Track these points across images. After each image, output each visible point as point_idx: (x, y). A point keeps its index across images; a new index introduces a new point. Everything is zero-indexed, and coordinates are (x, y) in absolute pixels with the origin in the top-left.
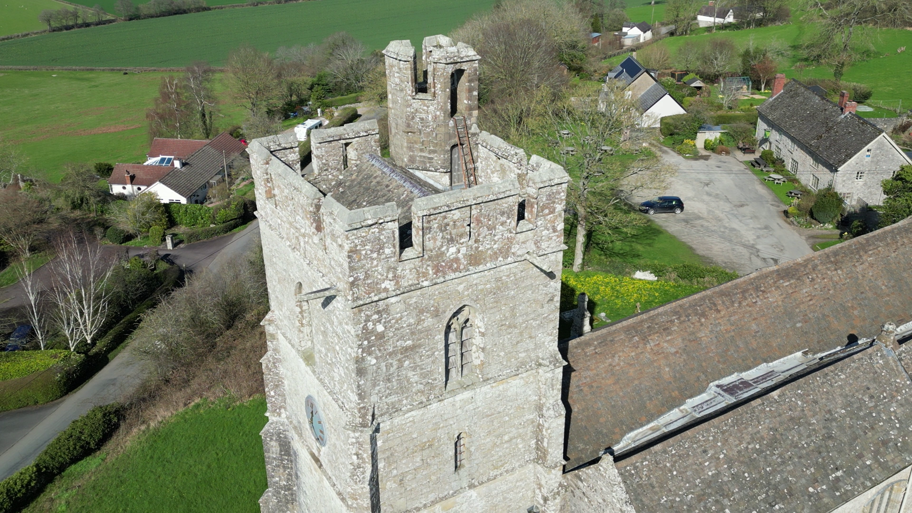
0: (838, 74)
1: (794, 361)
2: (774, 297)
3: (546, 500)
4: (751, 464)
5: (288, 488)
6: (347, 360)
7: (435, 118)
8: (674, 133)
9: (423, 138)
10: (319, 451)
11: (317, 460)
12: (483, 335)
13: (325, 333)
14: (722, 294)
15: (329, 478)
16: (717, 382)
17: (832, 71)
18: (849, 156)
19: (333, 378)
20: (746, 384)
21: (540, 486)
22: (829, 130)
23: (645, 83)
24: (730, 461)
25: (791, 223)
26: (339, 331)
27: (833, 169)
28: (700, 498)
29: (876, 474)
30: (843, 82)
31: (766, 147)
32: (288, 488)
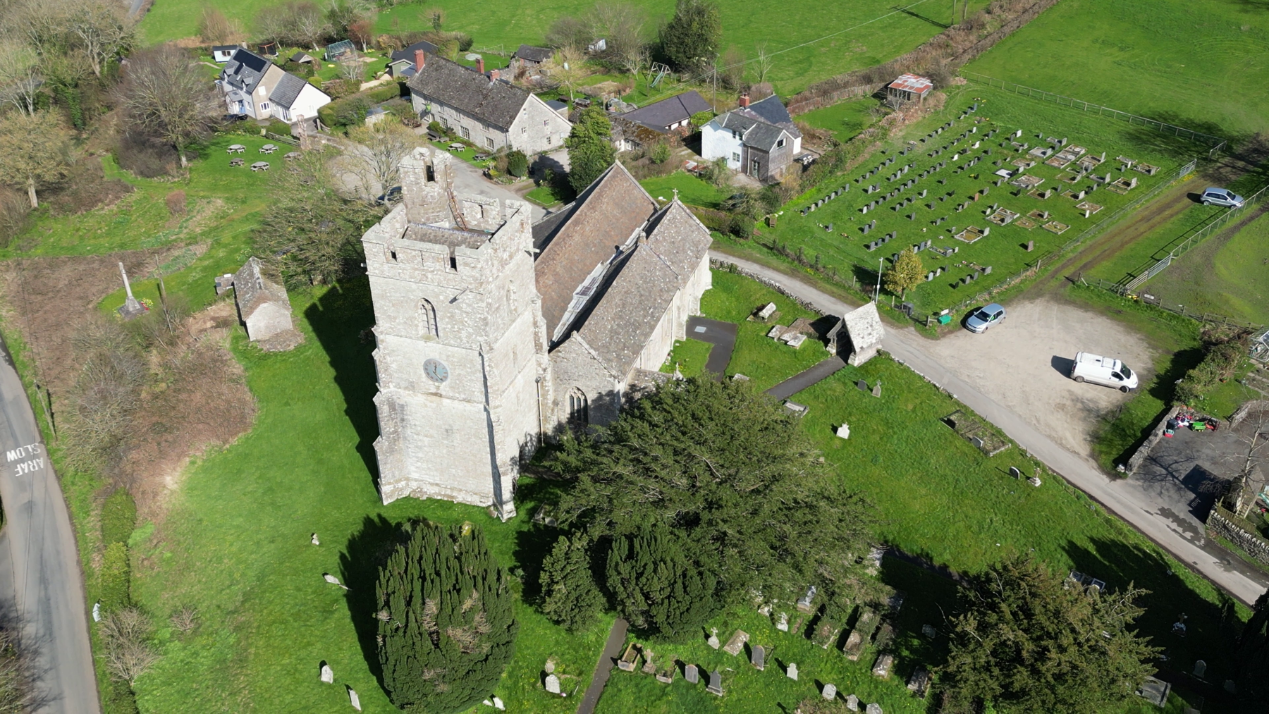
0: (437, 25)
2: (577, 238)
3: (545, 370)
4: (621, 317)
5: (395, 432)
8: (339, 120)
10: (438, 388)
11: (436, 394)
13: (452, 317)
15: (452, 398)
16: (579, 289)
17: (431, 24)
18: (513, 118)
20: (588, 288)
21: (540, 365)
22: (486, 97)
23: (274, 75)
25: (497, 183)
26: (469, 310)
27: (504, 130)
28: (611, 338)
29: (664, 305)
30: (444, 34)
31: (429, 120)
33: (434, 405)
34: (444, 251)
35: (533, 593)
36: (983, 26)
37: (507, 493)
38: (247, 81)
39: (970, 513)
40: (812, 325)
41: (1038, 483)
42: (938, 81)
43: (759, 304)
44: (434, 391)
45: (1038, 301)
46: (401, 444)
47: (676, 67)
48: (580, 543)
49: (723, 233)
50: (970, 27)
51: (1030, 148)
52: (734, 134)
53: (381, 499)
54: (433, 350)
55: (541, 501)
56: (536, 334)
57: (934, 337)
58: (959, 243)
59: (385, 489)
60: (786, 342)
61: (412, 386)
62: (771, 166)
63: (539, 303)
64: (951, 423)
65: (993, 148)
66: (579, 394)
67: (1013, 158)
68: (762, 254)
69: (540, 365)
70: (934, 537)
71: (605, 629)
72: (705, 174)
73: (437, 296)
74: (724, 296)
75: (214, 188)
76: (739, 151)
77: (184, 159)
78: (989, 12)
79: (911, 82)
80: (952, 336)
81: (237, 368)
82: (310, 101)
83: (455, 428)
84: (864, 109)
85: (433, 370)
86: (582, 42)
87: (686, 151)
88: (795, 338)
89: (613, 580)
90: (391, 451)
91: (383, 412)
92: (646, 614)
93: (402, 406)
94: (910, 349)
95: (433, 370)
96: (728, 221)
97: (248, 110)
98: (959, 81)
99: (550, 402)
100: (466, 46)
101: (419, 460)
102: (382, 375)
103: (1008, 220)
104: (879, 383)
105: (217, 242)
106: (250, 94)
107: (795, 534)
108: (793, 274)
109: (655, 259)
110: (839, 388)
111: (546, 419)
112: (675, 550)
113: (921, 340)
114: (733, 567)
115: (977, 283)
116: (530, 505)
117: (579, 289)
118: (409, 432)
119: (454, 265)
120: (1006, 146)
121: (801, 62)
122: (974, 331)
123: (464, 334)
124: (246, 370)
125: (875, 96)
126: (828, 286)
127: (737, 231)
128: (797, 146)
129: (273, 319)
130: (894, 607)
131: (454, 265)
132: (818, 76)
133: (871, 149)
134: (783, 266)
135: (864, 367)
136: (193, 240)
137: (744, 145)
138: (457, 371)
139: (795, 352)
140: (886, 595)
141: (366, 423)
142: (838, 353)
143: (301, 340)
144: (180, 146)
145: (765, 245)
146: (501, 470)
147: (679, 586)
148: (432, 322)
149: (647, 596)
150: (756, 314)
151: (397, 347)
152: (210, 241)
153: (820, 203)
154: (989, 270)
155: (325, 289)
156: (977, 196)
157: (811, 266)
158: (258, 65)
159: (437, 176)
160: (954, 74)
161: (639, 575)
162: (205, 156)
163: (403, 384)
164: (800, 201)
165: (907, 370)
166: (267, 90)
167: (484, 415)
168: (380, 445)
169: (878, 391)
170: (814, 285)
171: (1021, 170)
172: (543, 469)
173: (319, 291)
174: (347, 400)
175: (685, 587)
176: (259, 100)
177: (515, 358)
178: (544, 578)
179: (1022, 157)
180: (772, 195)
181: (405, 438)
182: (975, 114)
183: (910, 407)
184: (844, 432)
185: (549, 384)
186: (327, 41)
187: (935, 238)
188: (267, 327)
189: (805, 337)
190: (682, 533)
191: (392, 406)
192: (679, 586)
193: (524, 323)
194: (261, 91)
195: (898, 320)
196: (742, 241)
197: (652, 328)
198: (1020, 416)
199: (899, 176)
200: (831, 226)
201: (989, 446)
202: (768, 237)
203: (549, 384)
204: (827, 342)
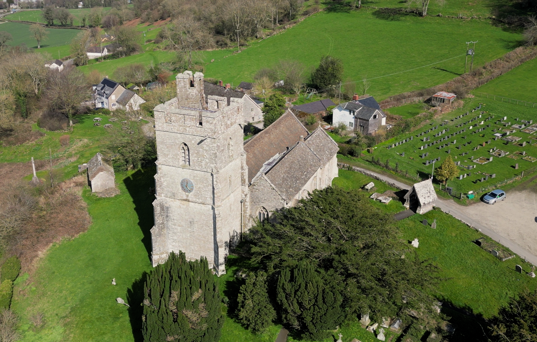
1: (277, 156)
3: (246, 195)
5: (163, 223)
6: (211, 155)
7: (196, 93)
9: (192, 100)
10: (187, 196)
11: (186, 200)
12: (232, 146)
13: (198, 153)
14: (255, 140)
16: (266, 163)
19: (201, 165)
20: (271, 163)
23: (120, 90)
24: (284, 173)
26: (207, 148)
28: (283, 181)
29: (313, 172)
32: (163, 223)
33: (185, 206)
34: (195, 113)
35: (233, 311)
36: (481, 74)
37: (221, 260)
38: (106, 92)
39: (493, 289)
40: (396, 193)
41: (534, 276)
42: (459, 95)
43: (364, 184)
44: (185, 198)
45: (524, 192)
46: (165, 231)
48: (262, 276)
49: (344, 155)
50: (474, 74)
51: (512, 125)
52: (350, 112)
53: (152, 264)
54: (186, 174)
55: (240, 266)
56: (242, 174)
57: (465, 205)
58: (475, 163)
59: (155, 257)
60: (380, 201)
61: (173, 196)
62: (370, 128)
63: (245, 156)
64: (478, 243)
65: (492, 124)
66: (264, 210)
67: (503, 129)
68: (367, 164)
69: (243, 192)
70: (472, 299)
73: (191, 141)
74: (345, 181)
75: (84, 135)
76: (353, 121)
77: (71, 122)
78: (484, 68)
79: (444, 94)
80: (475, 205)
81: (84, 204)
83: (195, 220)
84: (421, 108)
85: (186, 186)
87: (325, 123)
88: (386, 199)
89: (281, 296)
90: (160, 235)
91: (157, 210)
92: (300, 318)
93: (167, 208)
95: (186, 186)
97: (106, 106)
98: (470, 96)
99: (248, 215)
101: (174, 241)
102: (158, 189)
103: (503, 155)
104: (435, 221)
105: (82, 156)
106: (107, 98)
107: (391, 272)
108: (383, 173)
109: (308, 150)
110: (412, 224)
111: (245, 226)
112: (318, 279)
113: (458, 206)
114: (352, 290)
115: (487, 182)
116: (235, 268)
117: (266, 163)
118: (170, 223)
119: (201, 124)
121: (384, 89)
122: (488, 203)
123: (204, 163)
124: (88, 205)
125: (425, 102)
126: (403, 180)
127: (352, 153)
128: (384, 121)
129: (104, 181)
130: (449, 332)
131: (201, 124)
132: (394, 93)
133: (424, 123)
134: (378, 170)
135: (426, 215)
136: (70, 156)
137: (356, 118)
138: (199, 186)
139: (386, 206)
140: (444, 325)
141: (146, 218)
142: (410, 208)
143: (118, 193)
144: (70, 115)
145: (367, 161)
146: (219, 244)
147: (320, 298)
148: (187, 157)
149: (300, 304)
150: (363, 188)
151: (168, 174)
152: (78, 156)
153: (397, 144)
154: (494, 176)
155: (134, 172)
156: (484, 144)
157: (393, 170)
159: (196, 84)
160: (467, 92)
161: (296, 291)
162: (83, 122)
163: (169, 194)
164: (387, 143)
165: (451, 217)
166: (116, 97)
167: (211, 212)
168: (154, 231)
169: (434, 225)
170: (395, 179)
171: (508, 133)
172: (242, 250)
173: (130, 172)
174: (139, 219)
175: (324, 299)
176: (112, 101)
177: (230, 184)
178: (240, 298)
179: (508, 128)
180: (372, 141)
181: (167, 227)
182: (480, 110)
183: (454, 235)
184: (415, 243)
185: (248, 204)
187: (462, 161)
188: (102, 185)
189: (391, 199)
190: (322, 271)
191: (162, 207)
192: (320, 298)
195: (444, 196)
196: (354, 158)
197: (306, 181)
198: (519, 245)
199: (440, 135)
200: (404, 153)
201: (502, 255)
202: (369, 157)
203: (248, 204)
204: (403, 201)
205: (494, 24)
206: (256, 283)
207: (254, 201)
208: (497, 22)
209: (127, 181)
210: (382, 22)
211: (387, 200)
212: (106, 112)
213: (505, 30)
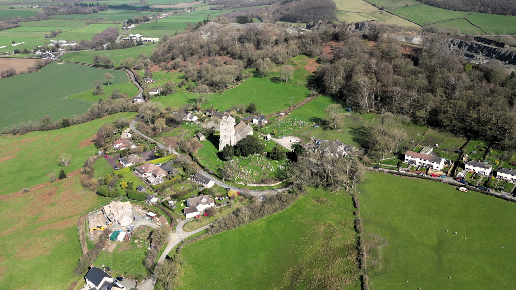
0: (212, 107)
8: (201, 120)
42: (286, 114)
47: (250, 113)
71: (241, 157)
72: (253, 125)
79: (282, 114)
82: (195, 118)
85: (225, 136)
86: (236, 109)
94: (275, 140)
96: (255, 129)
100: (217, 110)
120: (294, 121)
127: (257, 130)
128: (266, 122)
129: (203, 138)
132: (270, 113)
158: (187, 113)
172: (235, 147)
186: (192, 110)
193: (233, 132)
194: (188, 117)
205: (307, 87)
206: (238, 151)
207: (237, 138)
208: (307, 86)
209: (206, 138)
210: (273, 83)
211: (262, 139)
212: (188, 122)
213: (309, 89)
